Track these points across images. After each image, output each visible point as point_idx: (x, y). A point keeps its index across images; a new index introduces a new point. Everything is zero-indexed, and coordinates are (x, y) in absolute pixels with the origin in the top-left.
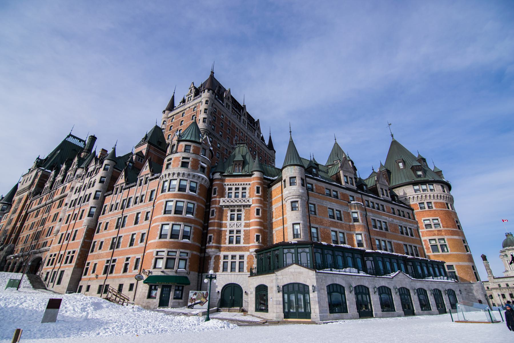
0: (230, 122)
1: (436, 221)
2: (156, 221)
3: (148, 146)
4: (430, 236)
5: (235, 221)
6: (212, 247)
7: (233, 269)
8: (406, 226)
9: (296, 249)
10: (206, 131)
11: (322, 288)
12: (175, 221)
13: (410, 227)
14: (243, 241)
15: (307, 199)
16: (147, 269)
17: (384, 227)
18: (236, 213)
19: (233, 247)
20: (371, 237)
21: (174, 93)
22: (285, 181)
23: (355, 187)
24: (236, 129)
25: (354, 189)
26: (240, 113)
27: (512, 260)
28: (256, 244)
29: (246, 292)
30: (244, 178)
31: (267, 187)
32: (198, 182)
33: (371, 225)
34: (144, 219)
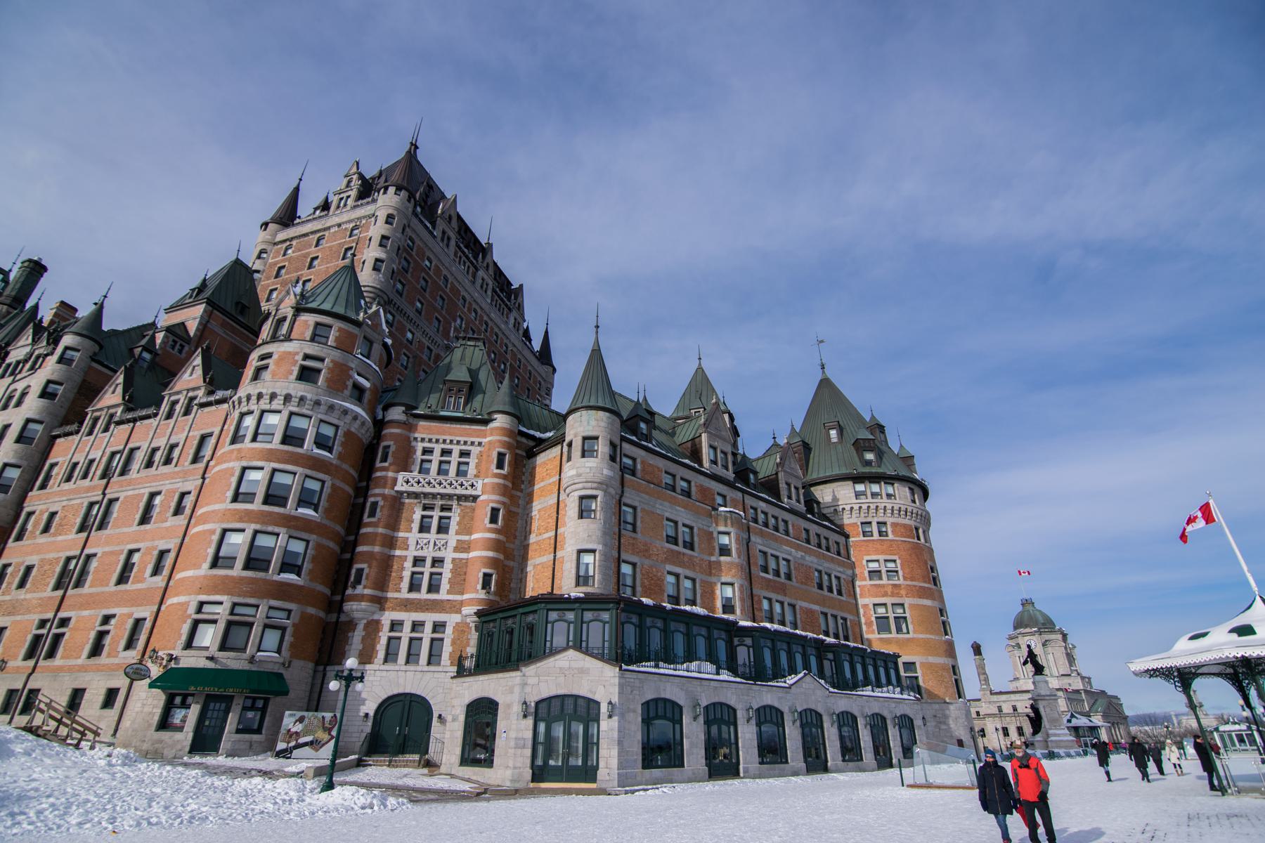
0: (446, 279)
1: (891, 565)
2: (205, 519)
3: (205, 311)
4: (877, 596)
5: (433, 536)
6: (361, 598)
7: (411, 657)
8: (829, 571)
9: (545, 611)
10: (380, 293)
11: (632, 707)
12: (263, 523)
13: (839, 575)
14: (448, 587)
15: (620, 492)
16: (163, 649)
17: (783, 570)
18: (436, 514)
19: (420, 600)
20: (754, 592)
21: (301, 180)
22: (570, 445)
23: (730, 475)
24: (461, 301)
25: (728, 478)
26: (477, 261)
27: (1028, 657)
28: (482, 595)
30: (468, 427)
31: (524, 454)
32: (341, 423)
33: (756, 564)
34: (172, 510)
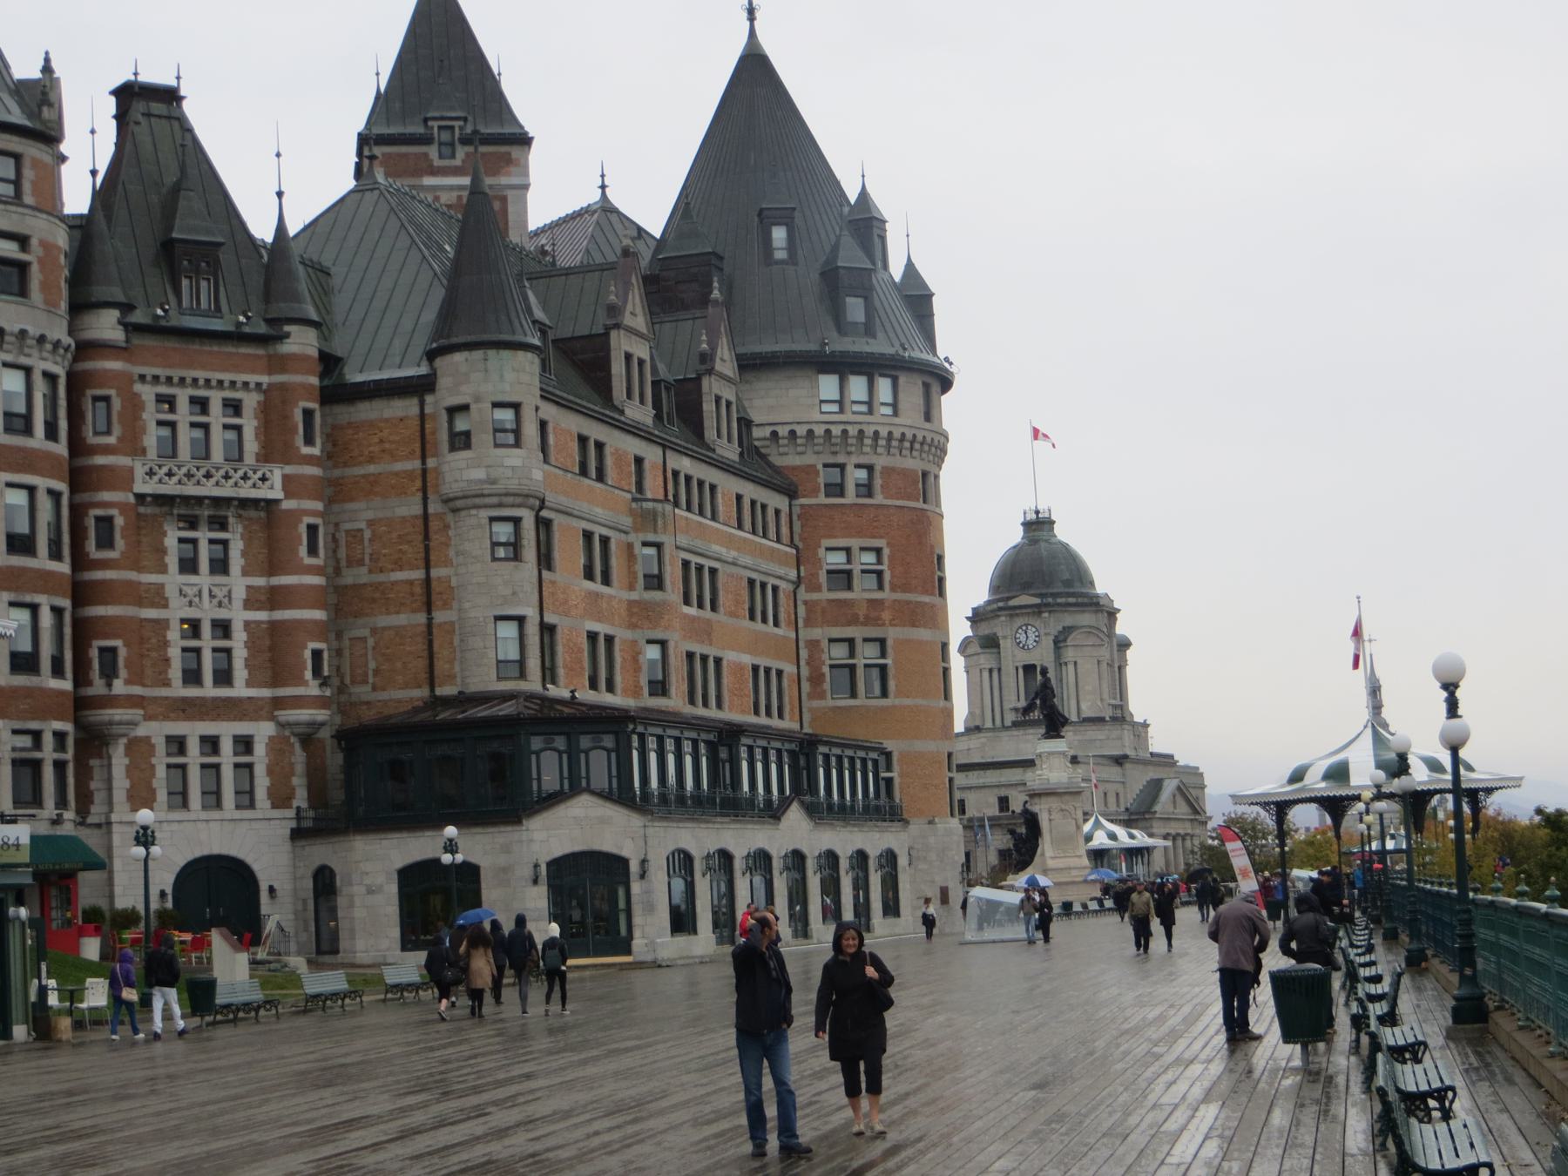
1: (869, 558)
4: (835, 624)
5: (204, 579)
7: (213, 797)
18: (203, 535)
19: (203, 699)
28: (312, 689)
29: (272, 890)
